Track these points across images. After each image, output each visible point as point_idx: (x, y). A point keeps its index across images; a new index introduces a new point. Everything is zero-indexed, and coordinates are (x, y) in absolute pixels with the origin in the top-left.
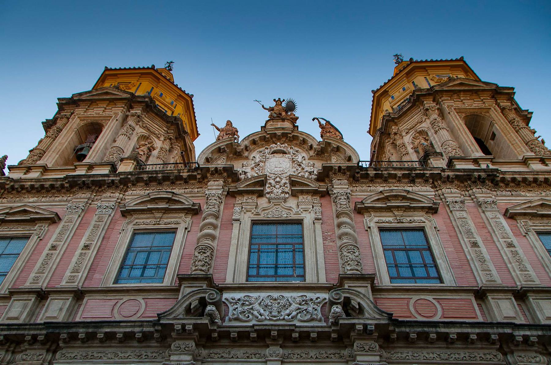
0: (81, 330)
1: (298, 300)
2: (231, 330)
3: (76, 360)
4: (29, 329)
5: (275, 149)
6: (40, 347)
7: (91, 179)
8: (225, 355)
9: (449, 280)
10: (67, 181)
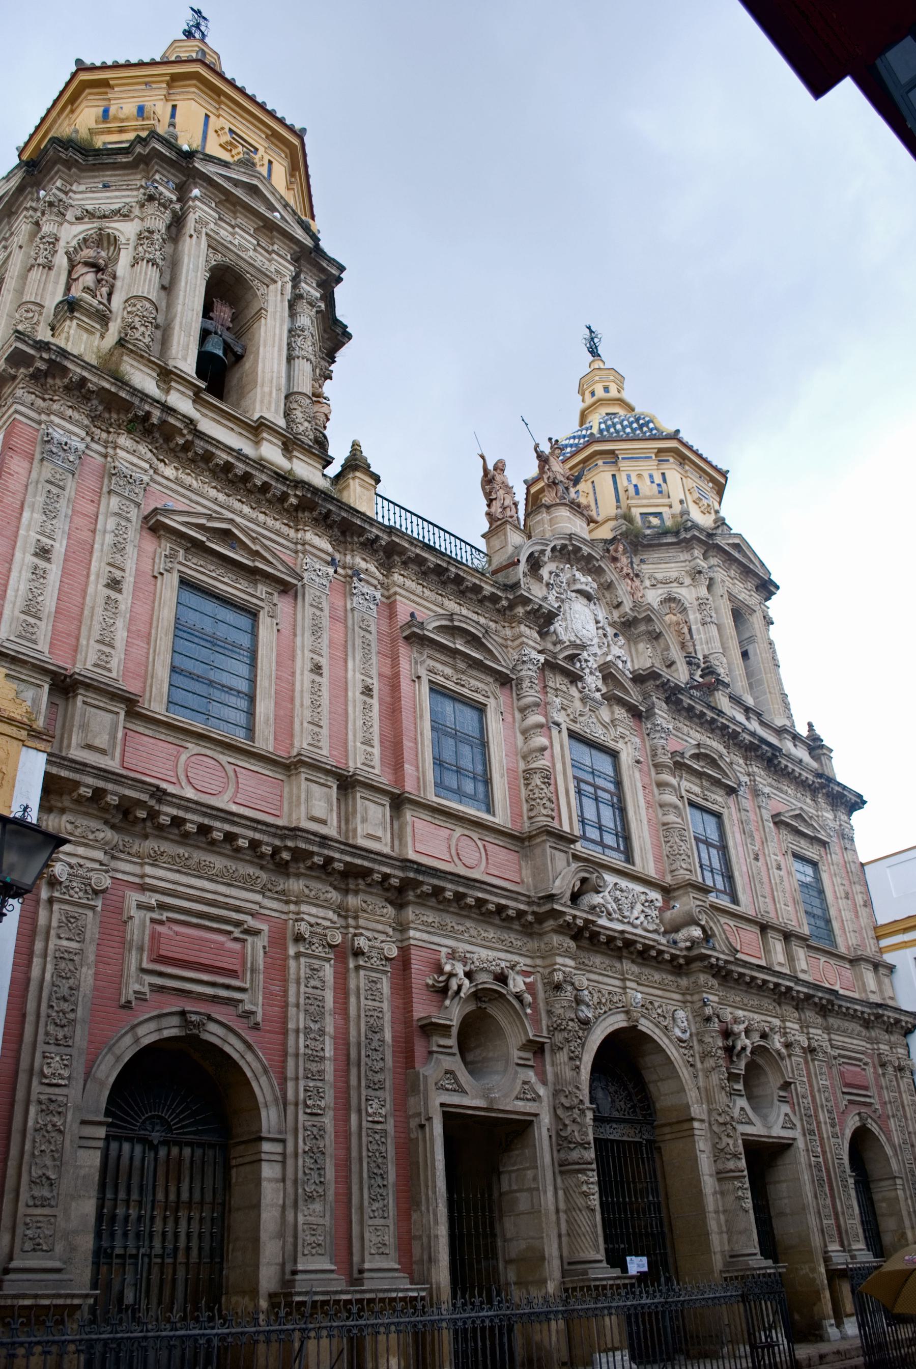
0: (449, 886)
1: (643, 897)
2: (602, 931)
3: (432, 930)
4: (381, 863)
5: (583, 587)
6: (380, 892)
7: (344, 514)
8: (587, 962)
9: (746, 906)
10: (298, 493)
